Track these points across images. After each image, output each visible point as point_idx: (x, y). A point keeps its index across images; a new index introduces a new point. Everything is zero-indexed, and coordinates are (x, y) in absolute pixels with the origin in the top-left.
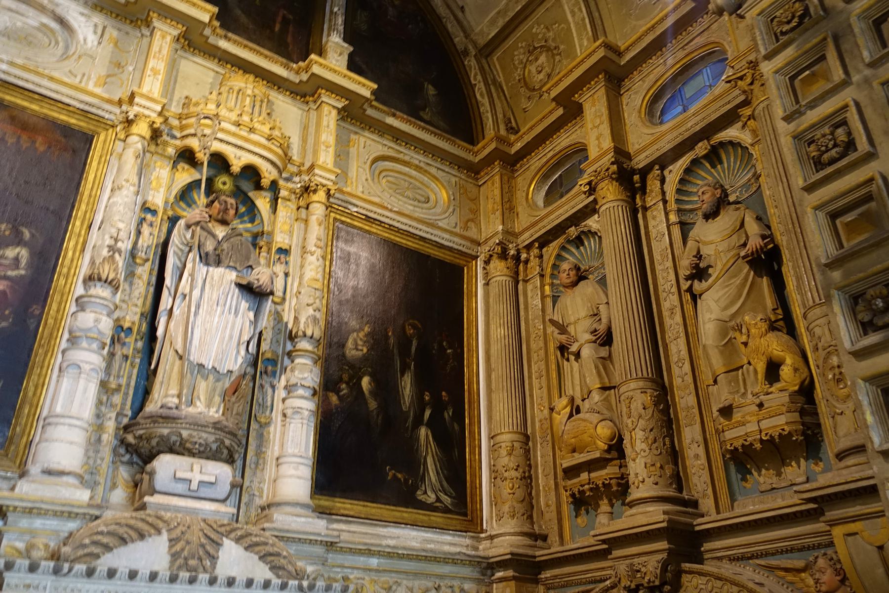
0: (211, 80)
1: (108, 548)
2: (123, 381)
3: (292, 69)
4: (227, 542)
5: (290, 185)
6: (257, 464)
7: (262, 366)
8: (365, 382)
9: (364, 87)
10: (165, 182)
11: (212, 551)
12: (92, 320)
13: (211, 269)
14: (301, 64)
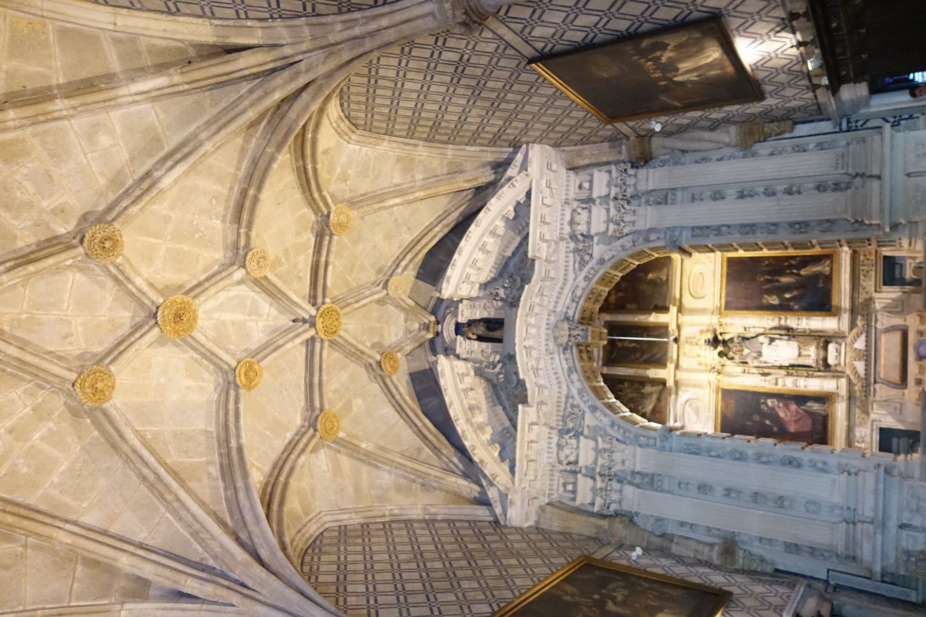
7: (790, 333)
8: (787, 296)
9: (673, 309)
10: (731, 367)
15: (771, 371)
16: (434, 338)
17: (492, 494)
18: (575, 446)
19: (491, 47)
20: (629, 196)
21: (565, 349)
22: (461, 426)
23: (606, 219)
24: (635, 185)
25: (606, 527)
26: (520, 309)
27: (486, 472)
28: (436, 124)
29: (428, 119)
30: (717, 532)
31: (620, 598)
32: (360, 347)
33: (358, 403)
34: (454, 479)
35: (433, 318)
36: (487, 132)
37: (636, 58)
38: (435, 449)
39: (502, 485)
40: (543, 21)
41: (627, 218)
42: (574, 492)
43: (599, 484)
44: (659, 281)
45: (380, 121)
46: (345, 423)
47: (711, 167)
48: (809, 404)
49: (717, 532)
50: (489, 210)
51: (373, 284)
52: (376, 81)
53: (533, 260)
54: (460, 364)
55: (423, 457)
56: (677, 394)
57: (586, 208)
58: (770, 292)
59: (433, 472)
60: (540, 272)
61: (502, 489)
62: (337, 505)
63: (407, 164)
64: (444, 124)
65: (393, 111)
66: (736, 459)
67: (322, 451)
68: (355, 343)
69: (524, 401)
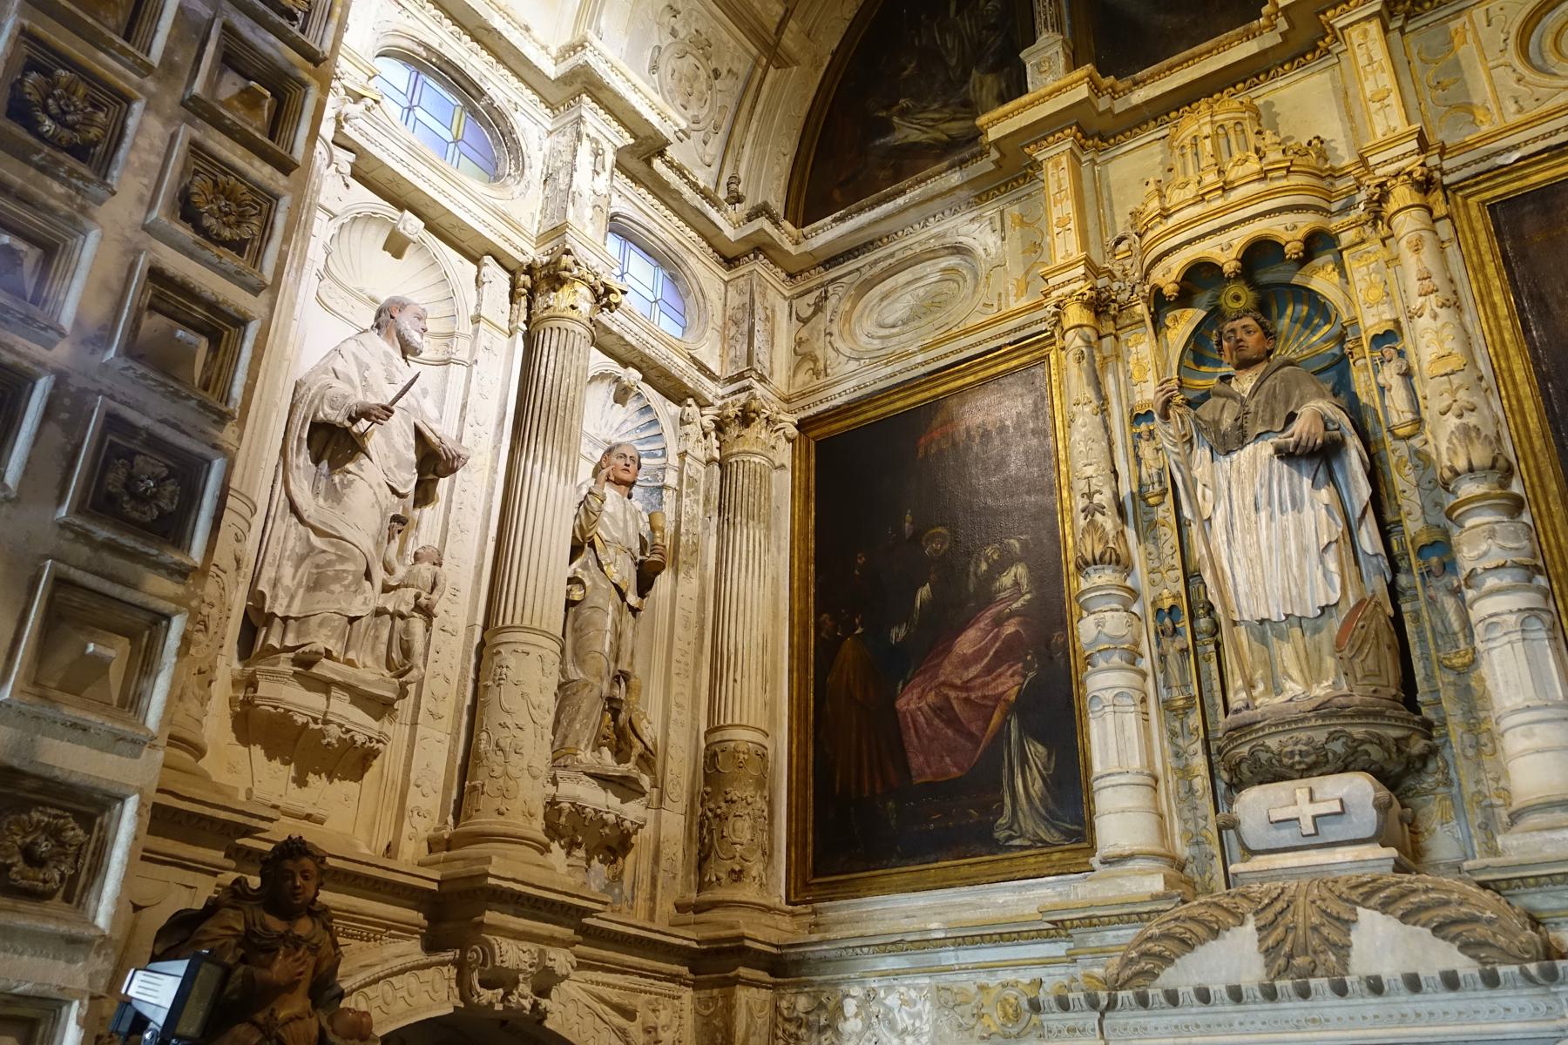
0: (1159, 158)
1: (1169, 961)
2: (1194, 690)
3: (1261, 29)
4: (1367, 917)
5: (1353, 215)
6: (1477, 746)
10: (1147, 362)
11: (1334, 937)
12: (1093, 626)
13: (1235, 456)
14: (1265, 10)
15: (1169, 536)
48: (1036, 751)
56: (982, 192)
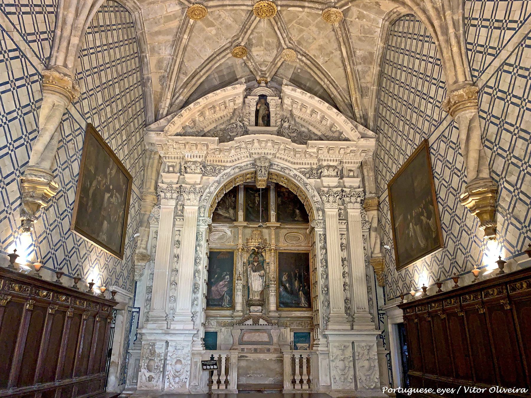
7: (266, 287)
9: (278, 224)
10: (246, 257)
16: (257, 80)
17: (162, 122)
18: (196, 171)
19: (436, 117)
20: (344, 199)
21: (253, 164)
22: (202, 101)
23: (331, 186)
24: (351, 202)
25: (150, 191)
26: (276, 136)
27: (176, 118)
28: (393, 80)
29: (396, 74)
30: (154, 251)
31: (113, 200)
32: (249, 32)
33: (212, 31)
34: (169, 97)
35: (269, 80)
36: (386, 113)
37: (424, 203)
38: (186, 84)
39: (169, 128)
40: (448, 148)
41: (331, 198)
42: (168, 172)
43: (175, 186)
44: (295, 216)
45: (396, 41)
46: (200, 23)
47: (361, 245)
48: (228, 297)
49: (154, 251)
50: (337, 115)
51: (290, 38)
52: (421, 41)
53: (306, 143)
54: (241, 100)
55: (181, 76)
56: (230, 227)
57: (337, 174)
58: (289, 276)
59: (172, 83)
60: (298, 148)
61: (166, 128)
62: (146, 20)
63: (368, 59)
64: (392, 84)
65: (402, 51)
66: (195, 260)
67: (180, 8)
68: (252, 28)
69: (221, 141)
